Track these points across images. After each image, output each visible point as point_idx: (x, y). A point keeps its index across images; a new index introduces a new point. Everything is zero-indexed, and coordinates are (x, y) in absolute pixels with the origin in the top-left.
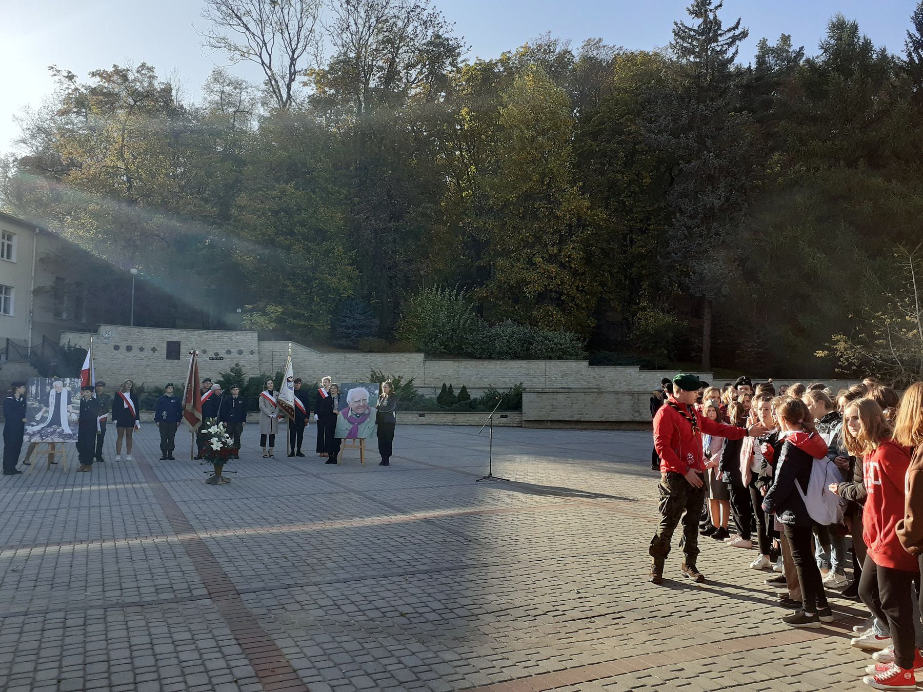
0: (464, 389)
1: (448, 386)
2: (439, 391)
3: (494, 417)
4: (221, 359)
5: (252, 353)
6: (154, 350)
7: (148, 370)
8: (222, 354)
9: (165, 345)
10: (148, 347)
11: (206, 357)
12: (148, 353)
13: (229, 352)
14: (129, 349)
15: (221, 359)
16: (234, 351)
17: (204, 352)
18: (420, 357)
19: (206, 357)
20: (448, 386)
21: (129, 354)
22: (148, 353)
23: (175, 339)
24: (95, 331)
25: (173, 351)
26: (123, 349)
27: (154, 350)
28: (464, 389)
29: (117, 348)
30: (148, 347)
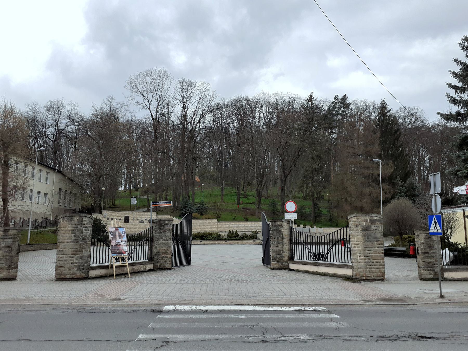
0: (236, 232)
1: (231, 231)
2: (227, 233)
3: (251, 241)
8: (144, 220)
11: (138, 222)
17: (138, 220)
18: (216, 220)
19: (138, 222)
20: (231, 231)
23: (128, 215)
24: (101, 213)
25: (127, 220)
26: (110, 219)
27: (120, 219)
28: (236, 232)
29: (108, 219)
30: (118, 218)
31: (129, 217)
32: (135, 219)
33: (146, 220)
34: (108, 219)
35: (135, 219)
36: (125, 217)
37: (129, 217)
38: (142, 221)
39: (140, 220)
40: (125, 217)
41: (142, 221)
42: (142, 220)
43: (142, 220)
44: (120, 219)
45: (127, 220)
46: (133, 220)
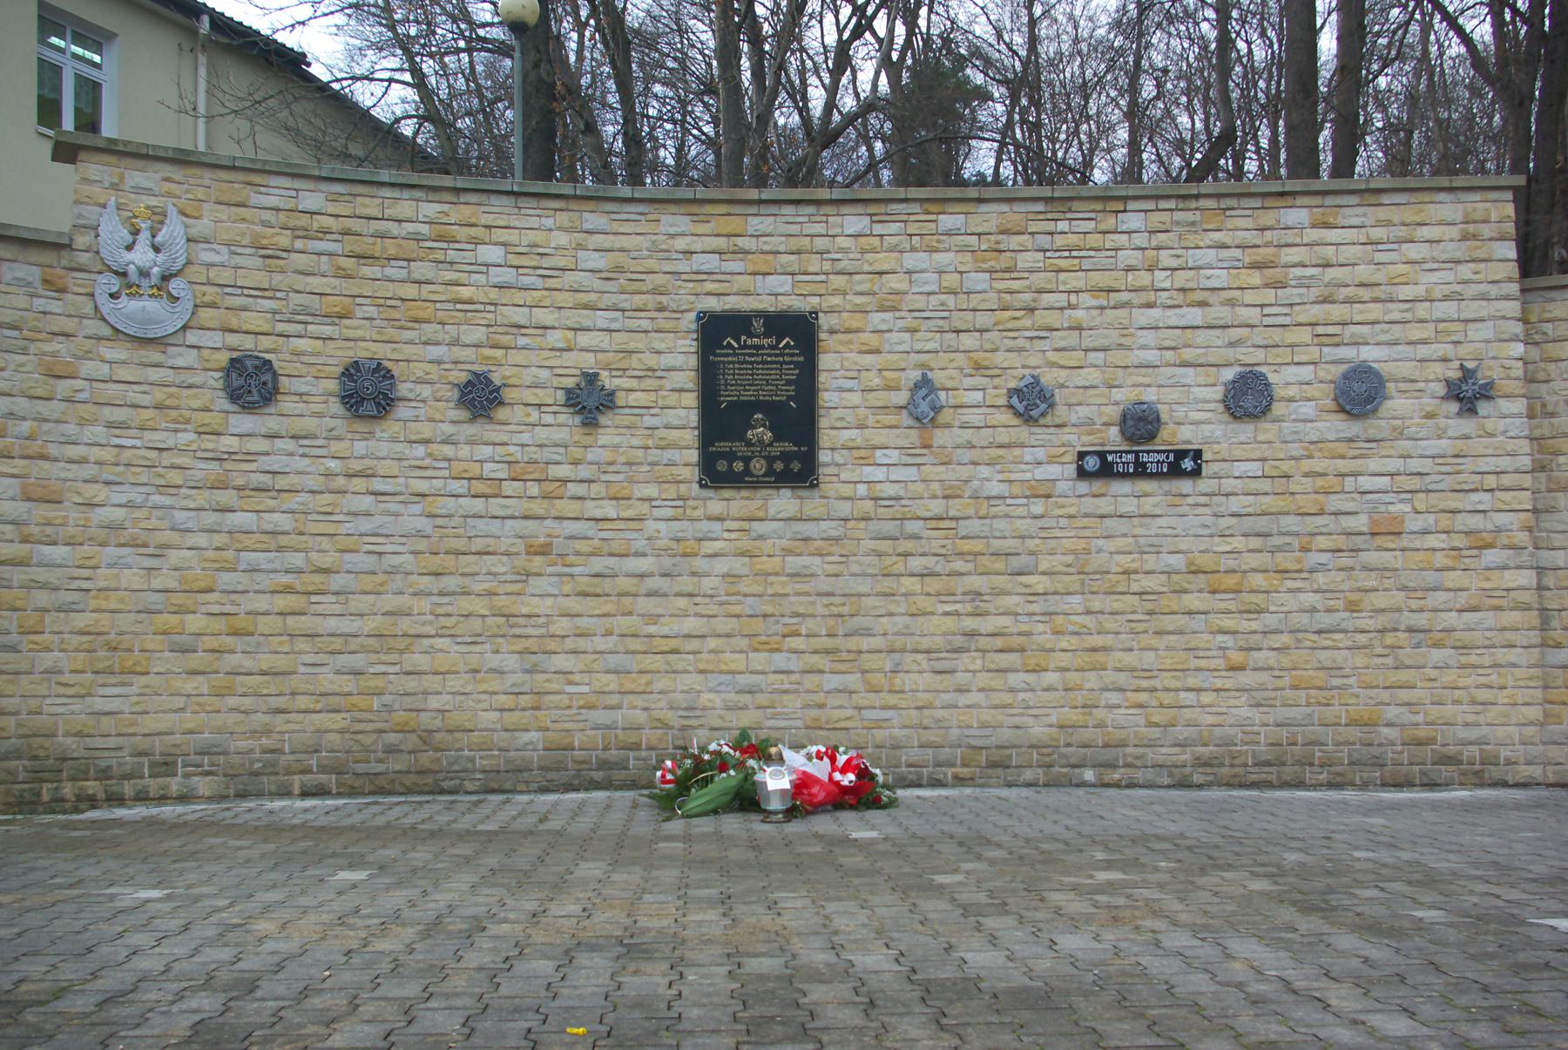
4: (1183, 464)
5: (1468, 393)
6: (589, 402)
7: (543, 597)
8: (1193, 416)
9: (682, 353)
10: (533, 376)
11: (1045, 457)
12: (535, 427)
13: (1248, 398)
14: (368, 393)
15: (1183, 464)
16: (1302, 386)
17: (1031, 402)
19: (1045, 457)
21: (379, 444)
22: (535, 427)
23: (773, 293)
26: (310, 396)
29: (252, 383)
31: (799, 331)
32: (976, 402)
33: (1248, 398)
34: (252, 383)
35: (976, 402)
36: (717, 331)
37: (799, 331)
38: (1142, 453)
39: (1091, 417)
40: (717, 331)
41: (1142, 453)
42: (1141, 423)
43: (1141, 423)
44: (589, 402)
45: (760, 409)
46: (924, 406)
